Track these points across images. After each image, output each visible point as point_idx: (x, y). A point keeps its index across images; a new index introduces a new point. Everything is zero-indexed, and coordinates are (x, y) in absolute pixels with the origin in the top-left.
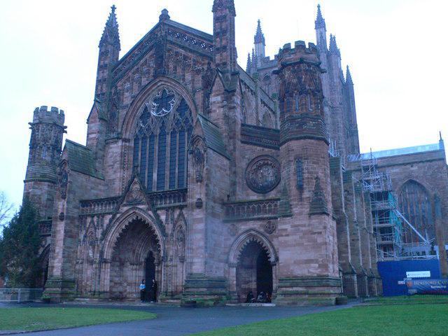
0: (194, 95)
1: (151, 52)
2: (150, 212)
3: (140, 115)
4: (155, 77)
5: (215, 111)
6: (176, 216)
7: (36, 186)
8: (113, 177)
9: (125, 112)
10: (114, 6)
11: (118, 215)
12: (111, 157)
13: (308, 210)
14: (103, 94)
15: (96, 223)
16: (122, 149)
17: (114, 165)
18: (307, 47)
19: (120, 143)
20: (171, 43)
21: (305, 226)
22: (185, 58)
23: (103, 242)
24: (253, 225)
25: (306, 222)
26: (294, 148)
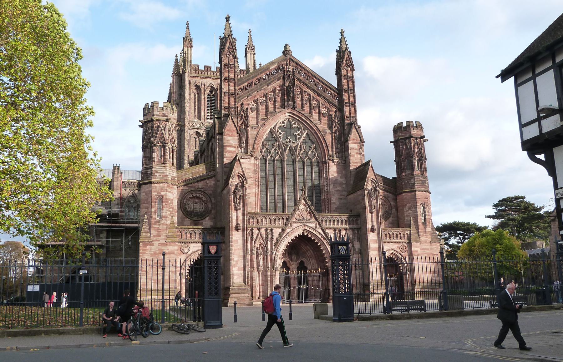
5: (354, 156)
7: (169, 190)
9: (255, 133)
13: (430, 239)
14: (232, 108)
18: (415, 125)
20: (300, 81)
21: (428, 249)
24: (393, 246)
25: (428, 247)
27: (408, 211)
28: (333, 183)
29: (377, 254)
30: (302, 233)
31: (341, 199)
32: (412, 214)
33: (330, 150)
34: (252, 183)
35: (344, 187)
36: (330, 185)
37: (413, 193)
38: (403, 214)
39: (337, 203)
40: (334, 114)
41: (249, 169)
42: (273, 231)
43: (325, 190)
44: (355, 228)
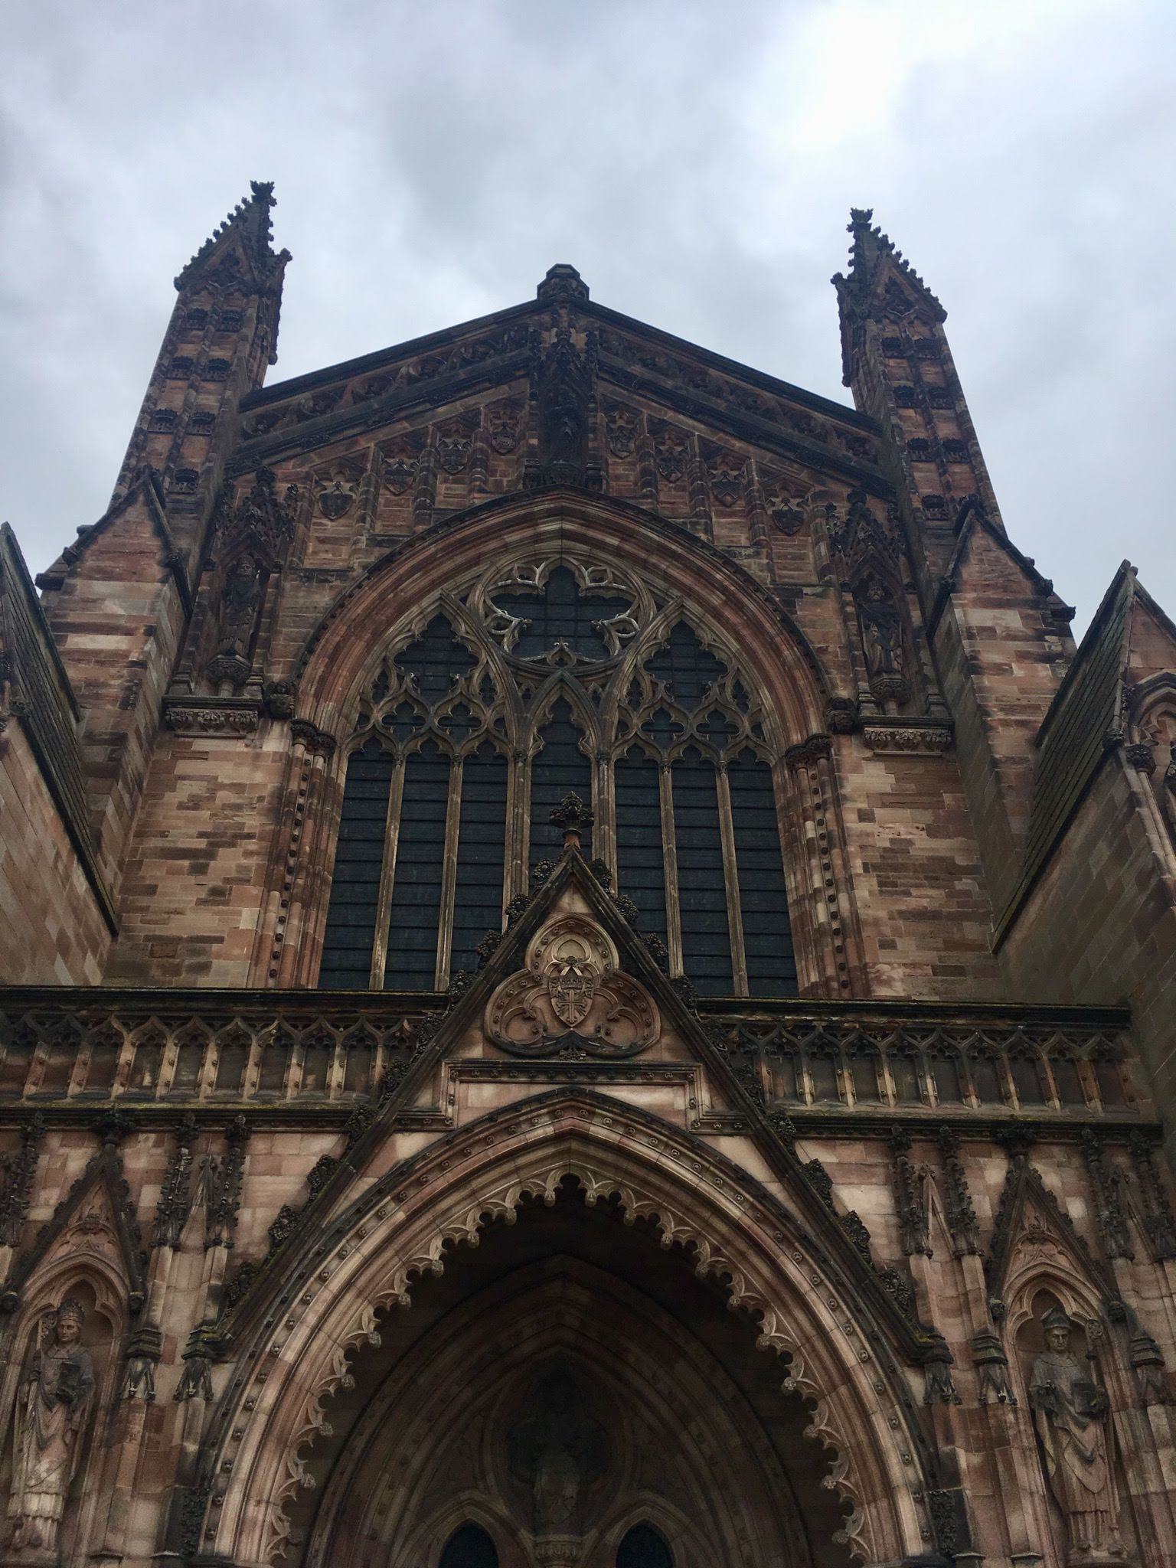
0: (791, 604)
1: (503, 392)
2: (736, 1150)
3: (400, 643)
4: (537, 483)
6: (984, 1206)
8: (205, 922)
9: (324, 599)
10: (269, 187)
11: (407, 1145)
12: (195, 803)
15: (148, 1197)
16: (286, 775)
17: (210, 854)
19: (275, 742)
22: (709, 452)
23: (220, 1378)
28: (876, 867)
31: (959, 971)
33: (836, 676)
34: (241, 868)
35: (967, 893)
36: (850, 880)
41: (238, 788)
42: (259, 1145)
44: (1103, 1130)
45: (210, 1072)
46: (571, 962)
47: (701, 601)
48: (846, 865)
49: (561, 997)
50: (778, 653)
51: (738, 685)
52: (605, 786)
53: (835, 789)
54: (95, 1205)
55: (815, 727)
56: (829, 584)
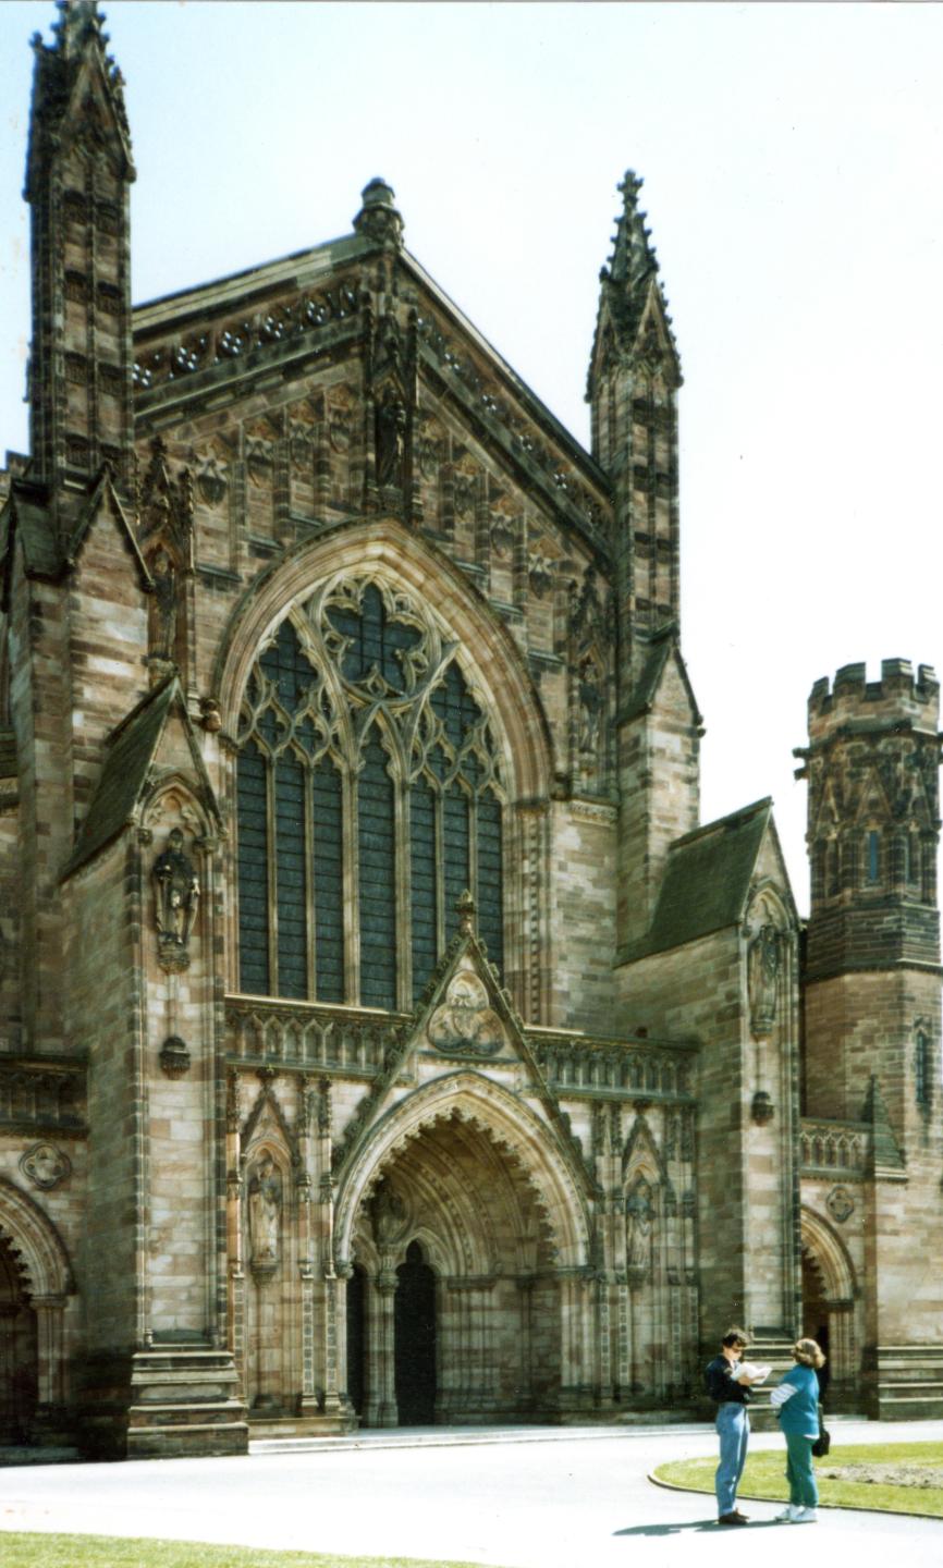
0: (537, 676)
15: (289, 1112)
26: (916, 994)
27: (861, 1050)
29: (769, 1220)
30: (450, 1111)
31: (594, 978)
32: (878, 1061)
33: (560, 749)
35: (605, 928)
36: (548, 911)
37: (890, 976)
38: (833, 1060)
39: (577, 996)
40: (581, 581)
42: (332, 1091)
43: (527, 931)
45: (304, 1050)
46: (463, 997)
47: (472, 650)
48: (548, 900)
49: (460, 1018)
50: (524, 717)
51: (488, 731)
52: (402, 808)
53: (548, 842)
54: (266, 1112)
55: (542, 791)
56: (562, 662)
